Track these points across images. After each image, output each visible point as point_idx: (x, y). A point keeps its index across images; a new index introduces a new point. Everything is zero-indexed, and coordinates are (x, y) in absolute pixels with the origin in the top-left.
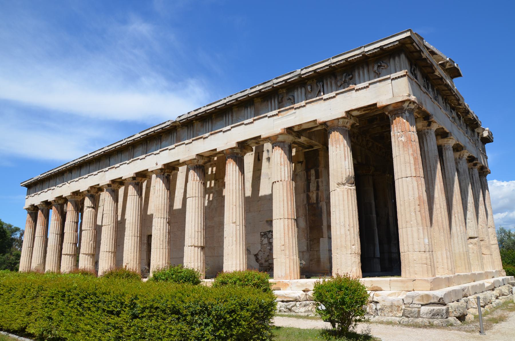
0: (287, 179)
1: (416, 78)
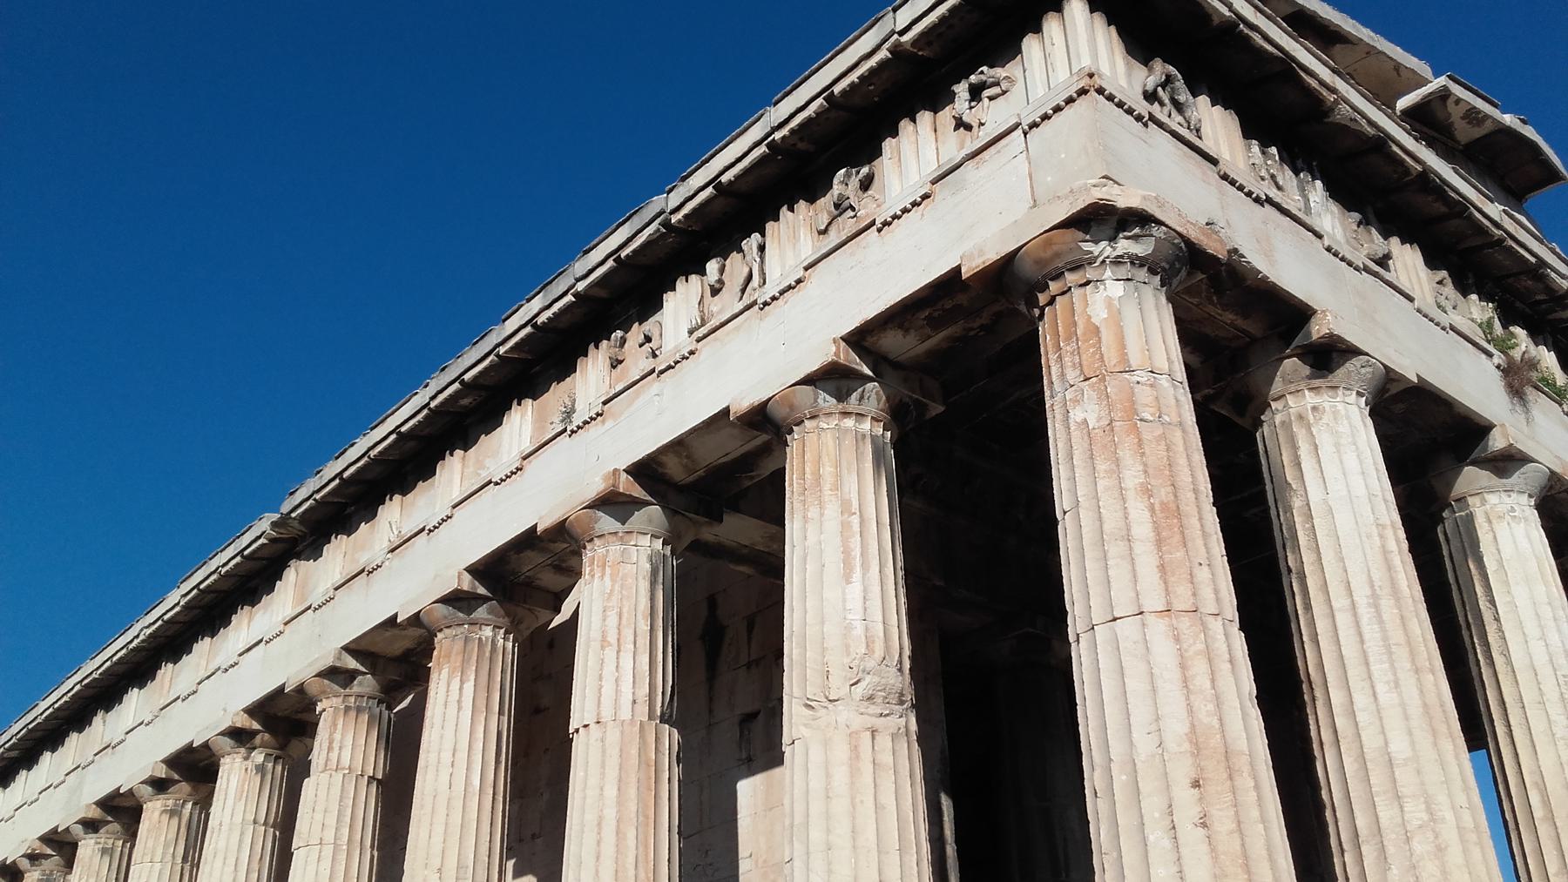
0: (625, 714)
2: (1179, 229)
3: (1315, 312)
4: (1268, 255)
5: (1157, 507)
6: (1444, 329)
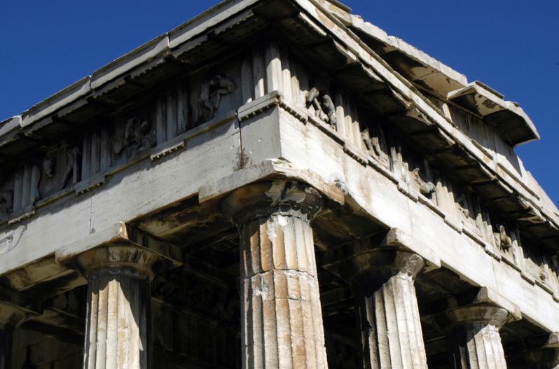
1: (329, 122)
2: (319, 188)
3: (389, 228)
4: (367, 198)
5: (294, 349)
6: (460, 232)
